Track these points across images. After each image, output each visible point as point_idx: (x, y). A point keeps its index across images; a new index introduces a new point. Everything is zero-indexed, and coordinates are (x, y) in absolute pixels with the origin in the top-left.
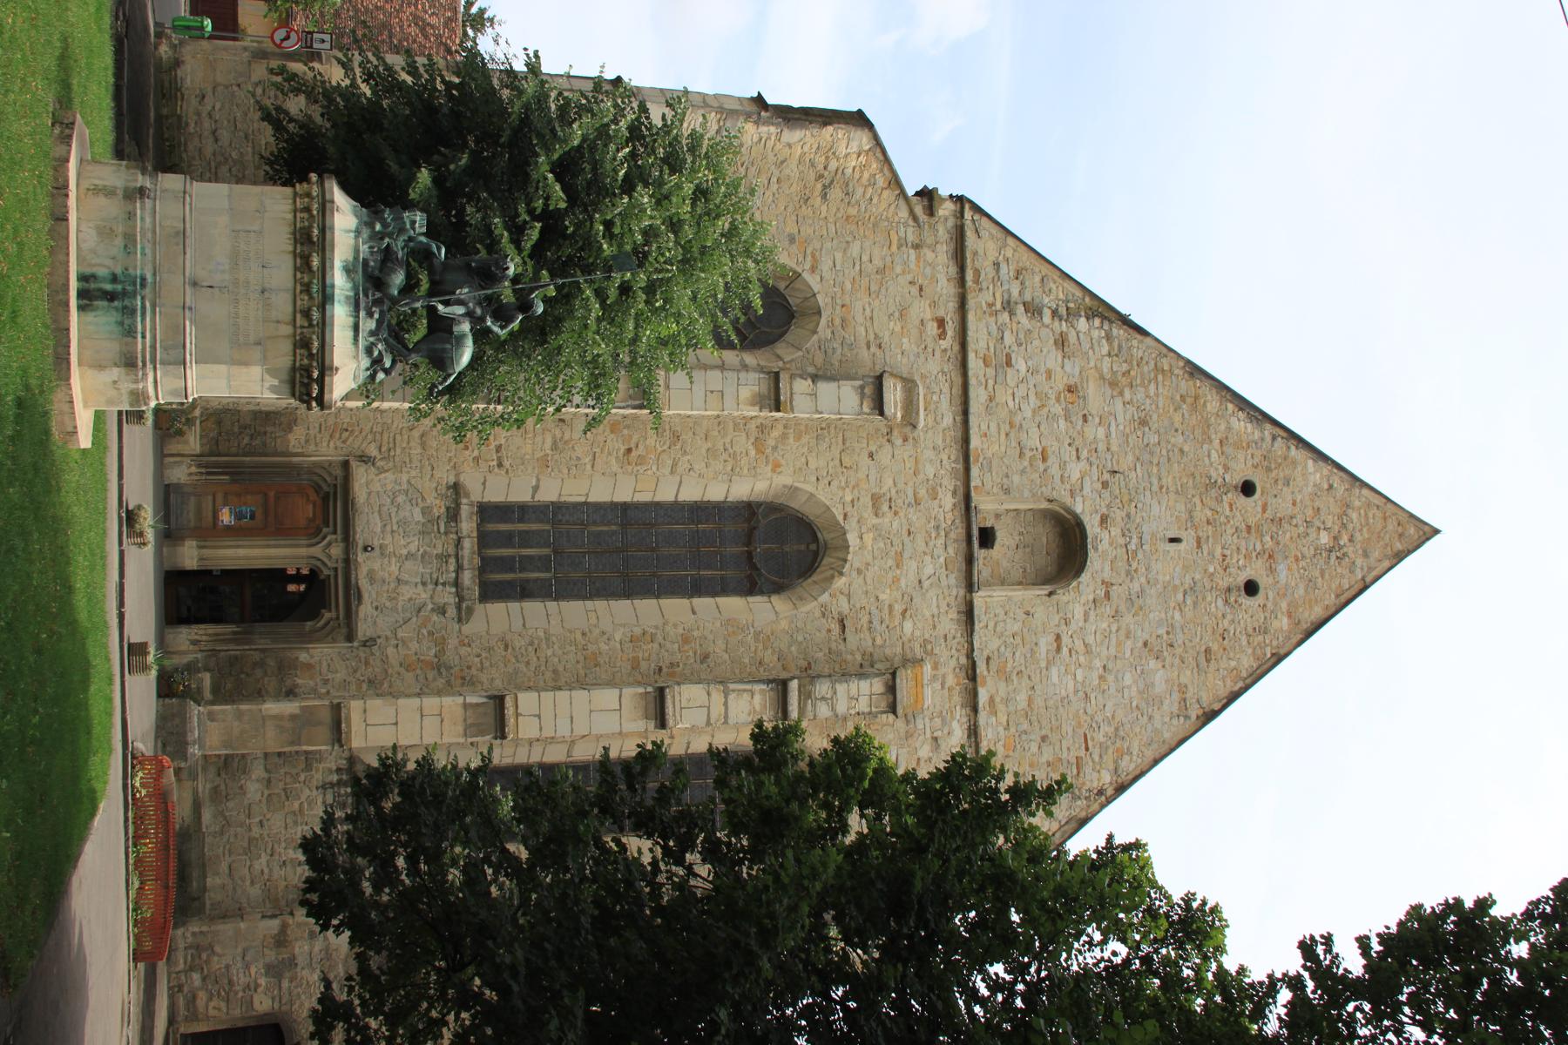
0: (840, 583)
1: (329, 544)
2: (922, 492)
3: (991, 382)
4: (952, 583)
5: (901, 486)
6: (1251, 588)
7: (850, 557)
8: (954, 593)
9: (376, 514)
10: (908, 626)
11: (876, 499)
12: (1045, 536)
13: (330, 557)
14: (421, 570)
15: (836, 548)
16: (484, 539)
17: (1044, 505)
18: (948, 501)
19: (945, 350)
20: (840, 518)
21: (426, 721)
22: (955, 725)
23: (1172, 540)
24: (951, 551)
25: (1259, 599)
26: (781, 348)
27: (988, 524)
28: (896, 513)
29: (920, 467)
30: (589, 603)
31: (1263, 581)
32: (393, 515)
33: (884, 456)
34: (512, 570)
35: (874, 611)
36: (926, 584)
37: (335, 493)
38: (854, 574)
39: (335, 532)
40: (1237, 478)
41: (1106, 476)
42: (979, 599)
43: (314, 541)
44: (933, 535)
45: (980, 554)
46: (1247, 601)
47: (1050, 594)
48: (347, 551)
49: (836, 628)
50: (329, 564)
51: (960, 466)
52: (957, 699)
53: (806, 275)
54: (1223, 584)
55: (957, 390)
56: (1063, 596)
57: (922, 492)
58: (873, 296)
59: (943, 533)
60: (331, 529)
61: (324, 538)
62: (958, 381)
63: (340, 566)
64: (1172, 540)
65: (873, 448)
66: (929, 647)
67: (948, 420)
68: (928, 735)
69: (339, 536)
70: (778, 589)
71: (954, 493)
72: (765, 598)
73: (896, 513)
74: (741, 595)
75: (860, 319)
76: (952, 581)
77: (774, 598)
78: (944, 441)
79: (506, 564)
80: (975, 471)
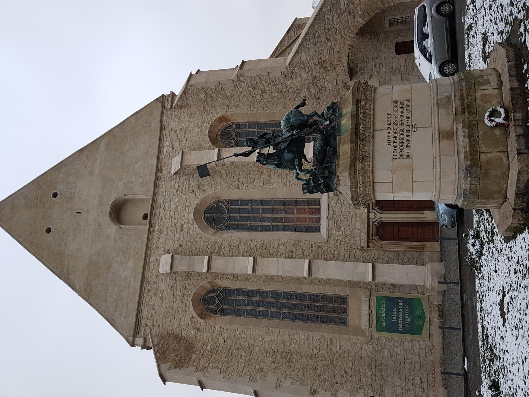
0: (197, 201)
2: (165, 232)
4: (160, 200)
5: (172, 235)
8: (159, 197)
9: (357, 229)
10: (177, 186)
11: (182, 229)
13: (375, 213)
16: (319, 220)
19: (149, 284)
20: (195, 223)
22: (165, 153)
26: (208, 286)
28: (175, 225)
29: (164, 241)
32: (351, 228)
33: (177, 245)
35: (188, 191)
36: (169, 200)
37: (372, 237)
38: (192, 204)
39: (372, 222)
43: (380, 220)
44: (164, 217)
48: (368, 216)
49: (202, 187)
50: (375, 211)
53: (195, 315)
57: (165, 232)
58: (172, 306)
59: (160, 218)
60: (374, 224)
61: (376, 220)
65: (180, 248)
66: (170, 179)
67: (152, 258)
68: (175, 150)
69: (371, 221)
73: (175, 225)
75: (178, 297)
76: (159, 201)
79: (311, 211)
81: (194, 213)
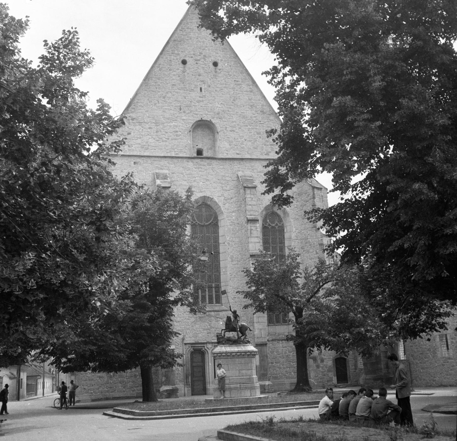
0: (216, 199)
1: (208, 348)
3: (154, 148)
6: (215, 64)
7: (208, 196)
12: (199, 132)
14: (214, 322)
15: (205, 200)
17: (191, 133)
18: (190, 164)
21: (260, 321)
23: (201, 89)
24: (205, 164)
25: (219, 62)
27: (196, 150)
30: (221, 274)
31: (213, 59)
34: (212, 296)
39: (204, 347)
40: (182, 65)
41: (182, 111)
42: (220, 156)
45: (205, 154)
46: (220, 65)
47: (218, 133)
48: (209, 343)
51: (180, 160)
52: (248, 165)
54: (214, 73)
55: (157, 159)
56: (219, 129)
61: (206, 349)
62: (154, 159)
63: (213, 345)
64: (201, 89)
69: (205, 345)
70: (216, 218)
71: (188, 162)
72: (219, 221)
74: (218, 229)
77: (219, 218)
78: (172, 164)
80: (181, 155)
81: (205, 196)
